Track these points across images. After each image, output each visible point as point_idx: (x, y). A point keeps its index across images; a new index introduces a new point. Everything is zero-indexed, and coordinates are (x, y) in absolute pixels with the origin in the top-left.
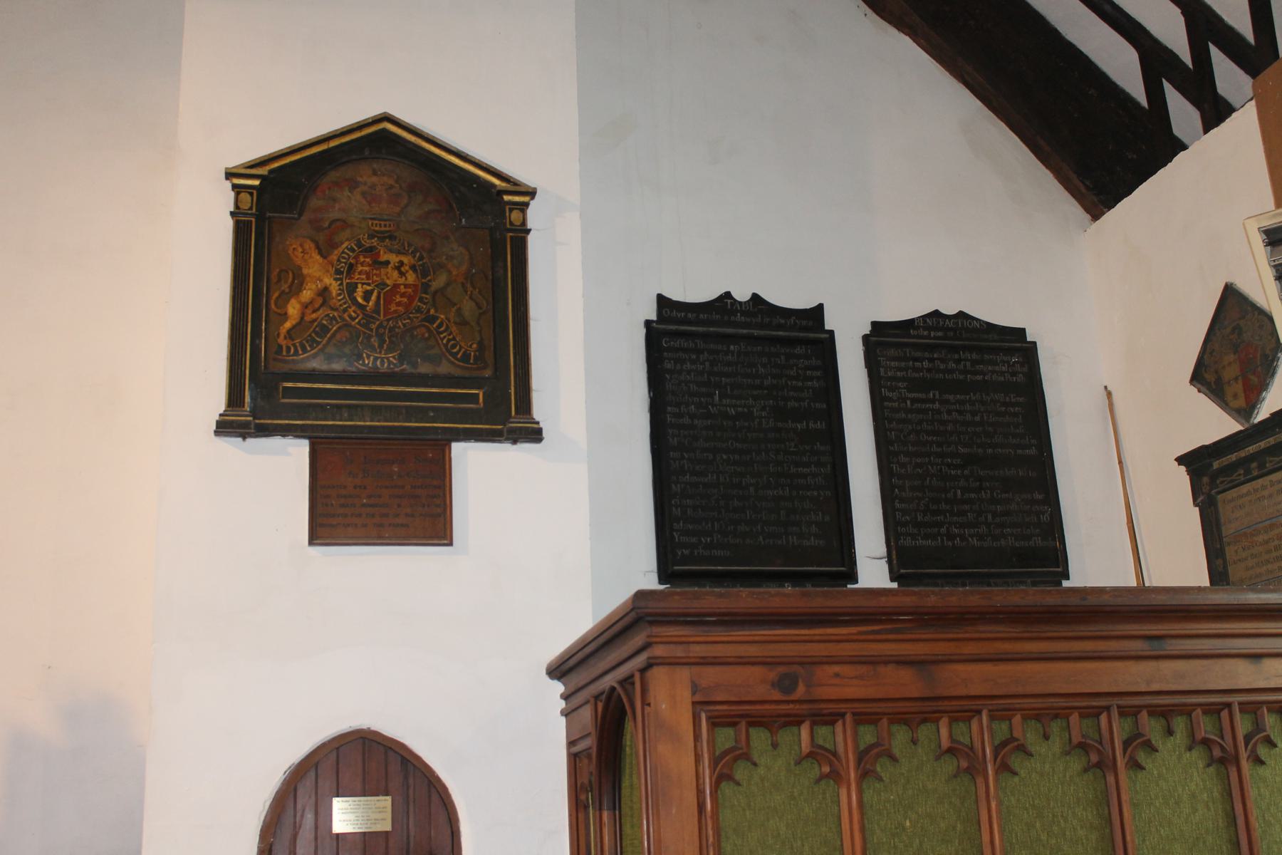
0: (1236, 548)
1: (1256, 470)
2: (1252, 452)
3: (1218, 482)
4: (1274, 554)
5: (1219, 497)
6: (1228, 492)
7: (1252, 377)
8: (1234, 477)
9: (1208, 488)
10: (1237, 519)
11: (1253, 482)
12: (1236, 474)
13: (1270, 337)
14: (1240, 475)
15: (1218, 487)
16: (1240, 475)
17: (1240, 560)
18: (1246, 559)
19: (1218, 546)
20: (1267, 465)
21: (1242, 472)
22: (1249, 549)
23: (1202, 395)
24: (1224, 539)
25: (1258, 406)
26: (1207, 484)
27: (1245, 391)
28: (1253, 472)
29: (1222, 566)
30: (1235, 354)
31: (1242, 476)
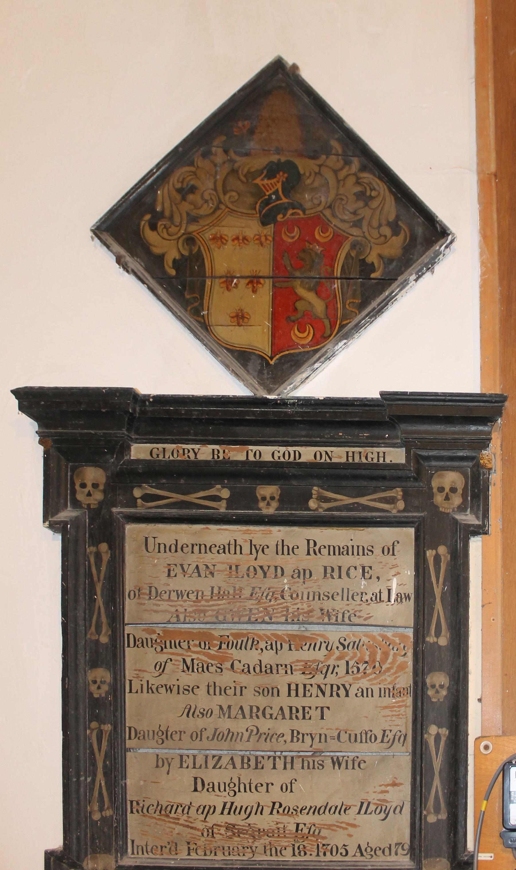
0: (163, 658)
1: (275, 504)
2: (267, 458)
3: (137, 493)
4: (284, 701)
5: (130, 528)
6: (161, 526)
7: (311, 296)
8: (191, 498)
9: (98, 496)
10: (180, 594)
11: (252, 528)
12: (202, 494)
13: (386, 231)
14: (216, 498)
15: (135, 506)
16: (216, 498)
17: (169, 689)
18: (191, 690)
19: (104, 639)
20: (312, 504)
21: (225, 494)
22: (205, 668)
23: (130, 280)
24: (128, 630)
25: (316, 365)
26: (95, 486)
27: (275, 317)
28: (262, 504)
29: (105, 688)
30: (264, 224)
31: (224, 504)
